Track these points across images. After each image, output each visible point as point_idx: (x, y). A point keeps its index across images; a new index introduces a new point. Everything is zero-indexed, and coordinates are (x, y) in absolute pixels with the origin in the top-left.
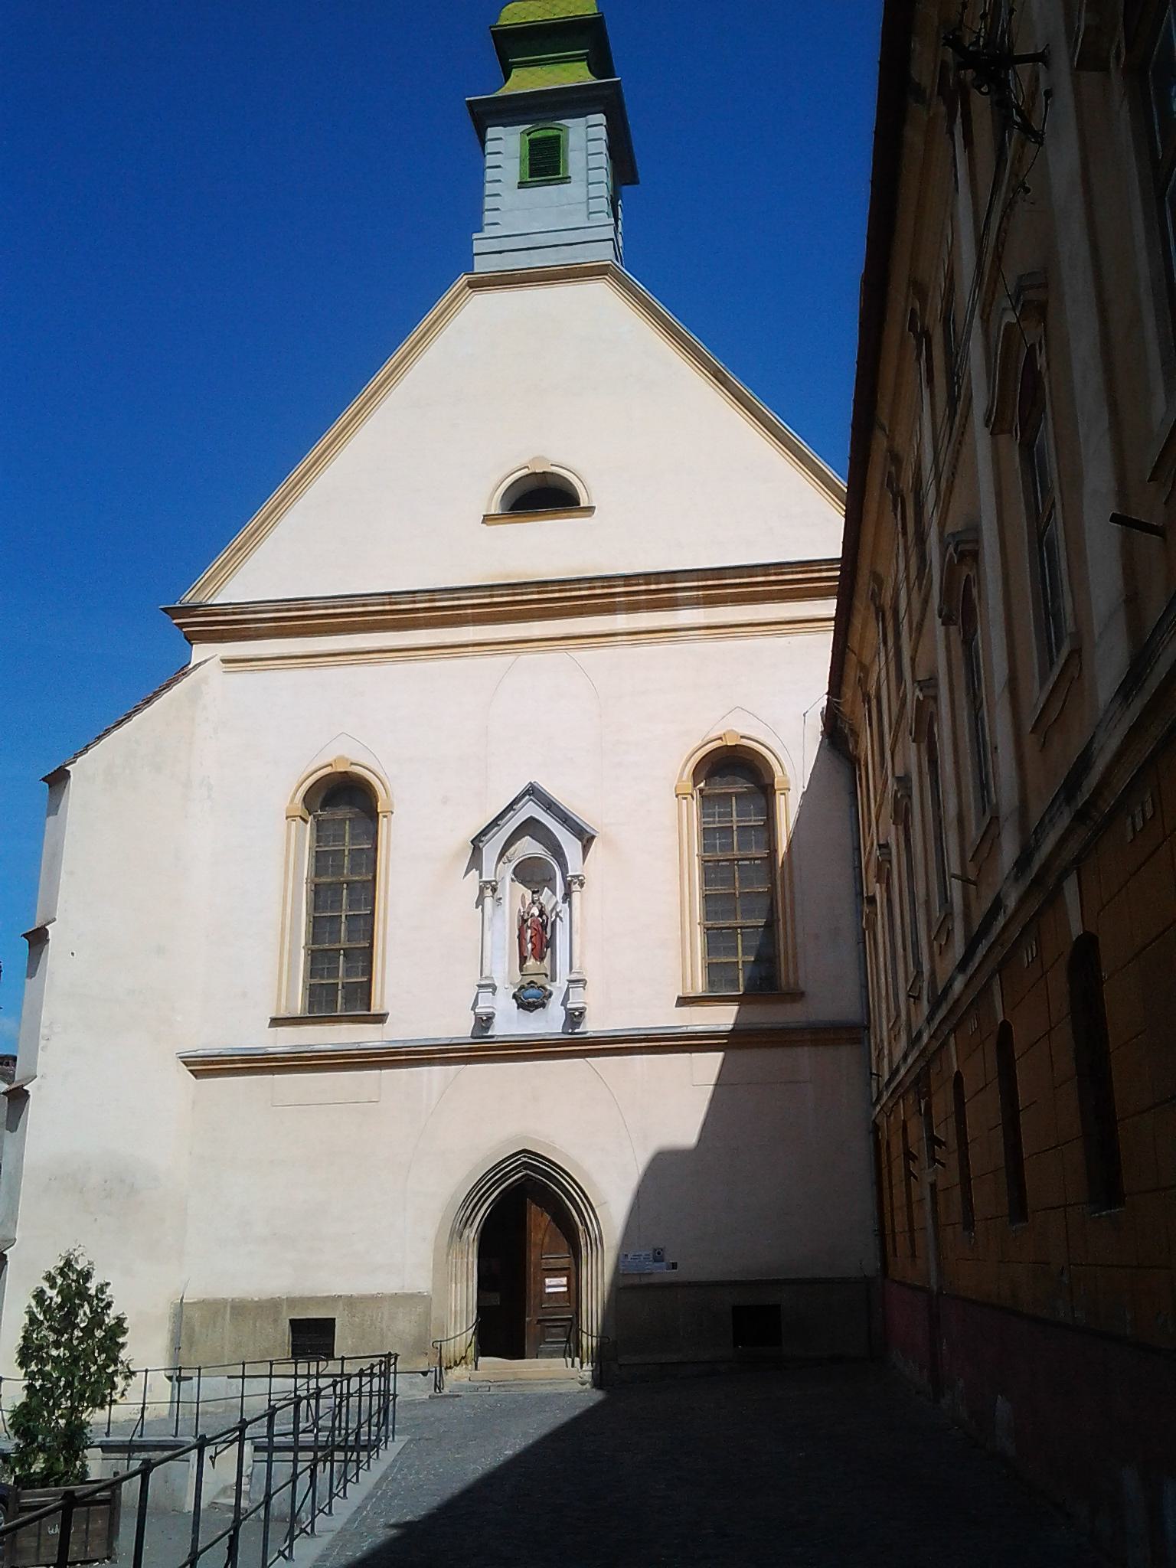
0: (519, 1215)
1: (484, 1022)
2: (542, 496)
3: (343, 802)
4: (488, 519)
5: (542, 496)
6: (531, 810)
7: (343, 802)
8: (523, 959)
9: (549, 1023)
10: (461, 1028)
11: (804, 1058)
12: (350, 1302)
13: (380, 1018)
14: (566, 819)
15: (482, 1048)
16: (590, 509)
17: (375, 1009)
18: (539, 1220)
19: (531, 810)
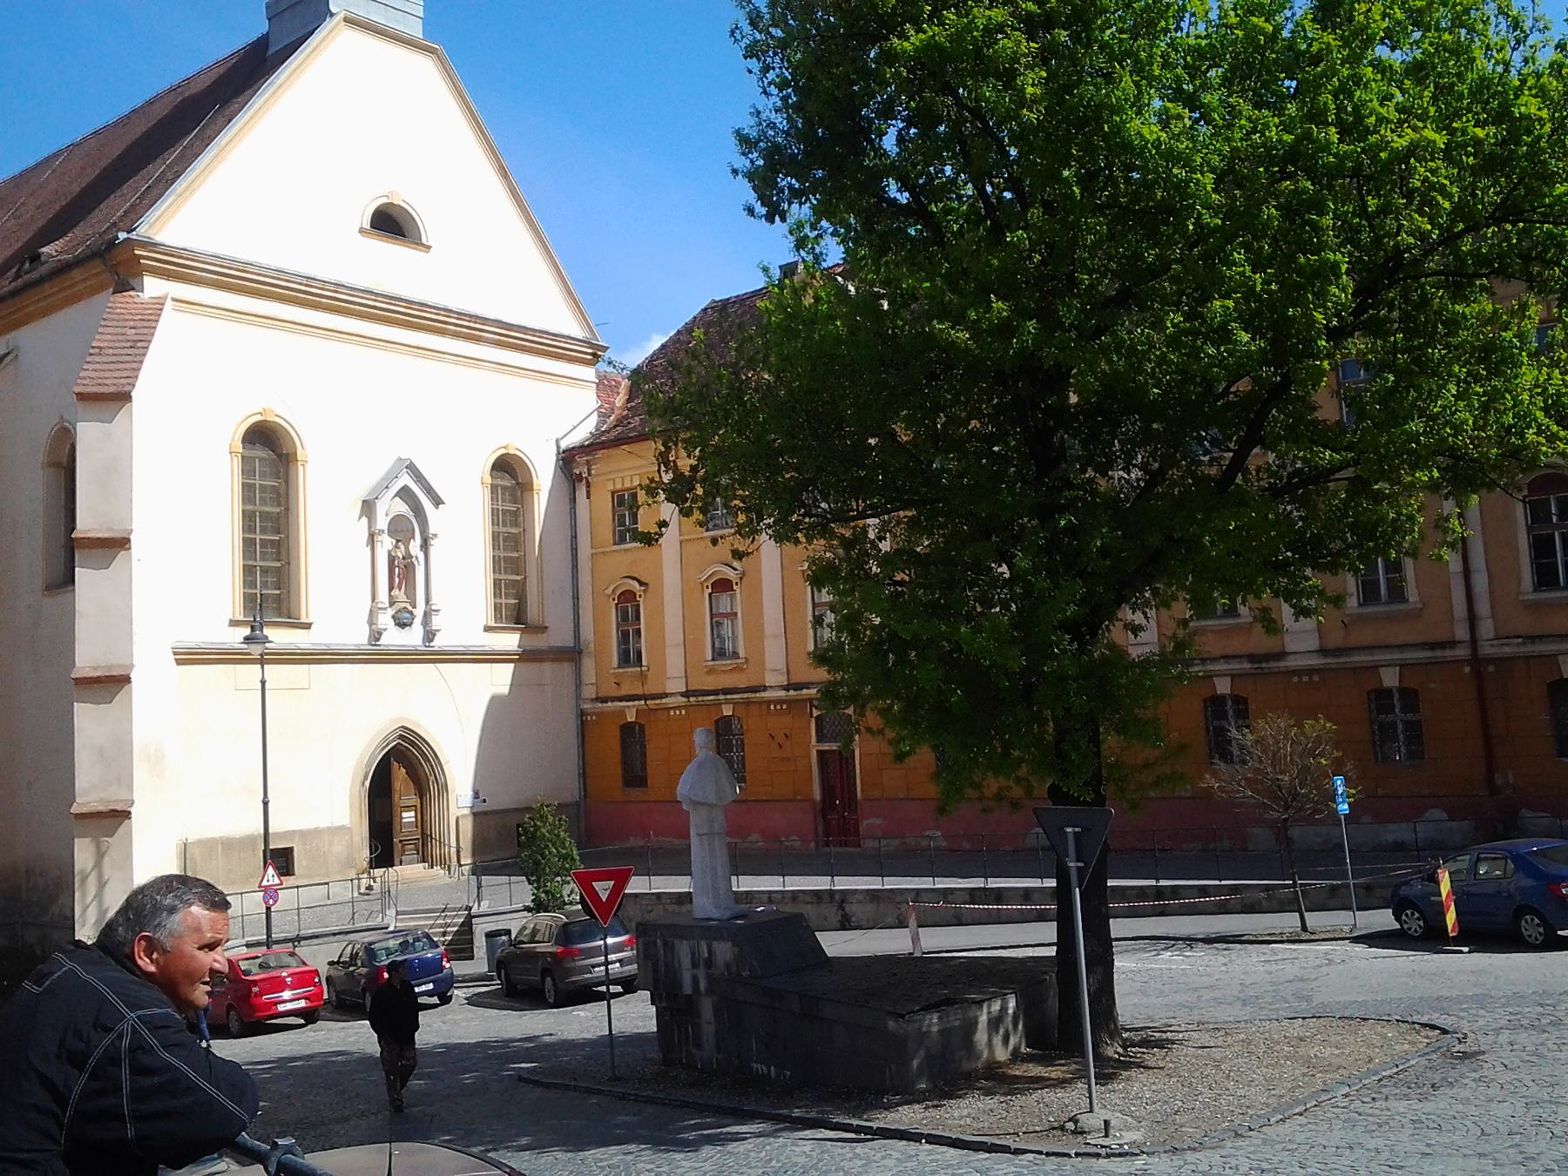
0: (400, 770)
1: (376, 635)
2: (391, 223)
3: (268, 448)
4: (362, 231)
5: (391, 223)
6: (406, 480)
7: (268, 448)
8: (391, 588)
9: (412, 637)
10: (358, 637)
11: (547, 668)
12: (303, 835)
13: (308, 626)
14: (429, 491)
15: (375, 655)
16: (429, 247)
17: (303, 620)
18: (400, 774)
19: (406, 480)
